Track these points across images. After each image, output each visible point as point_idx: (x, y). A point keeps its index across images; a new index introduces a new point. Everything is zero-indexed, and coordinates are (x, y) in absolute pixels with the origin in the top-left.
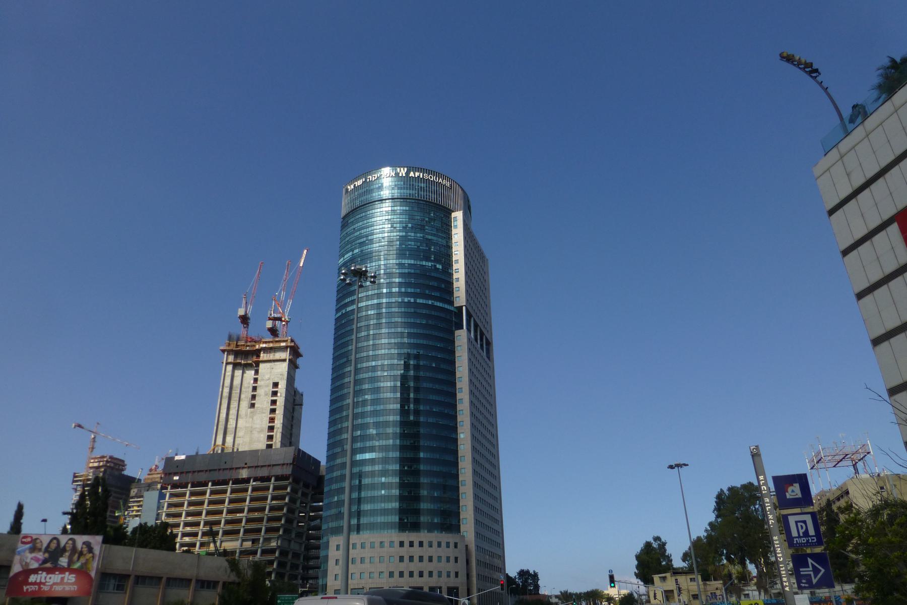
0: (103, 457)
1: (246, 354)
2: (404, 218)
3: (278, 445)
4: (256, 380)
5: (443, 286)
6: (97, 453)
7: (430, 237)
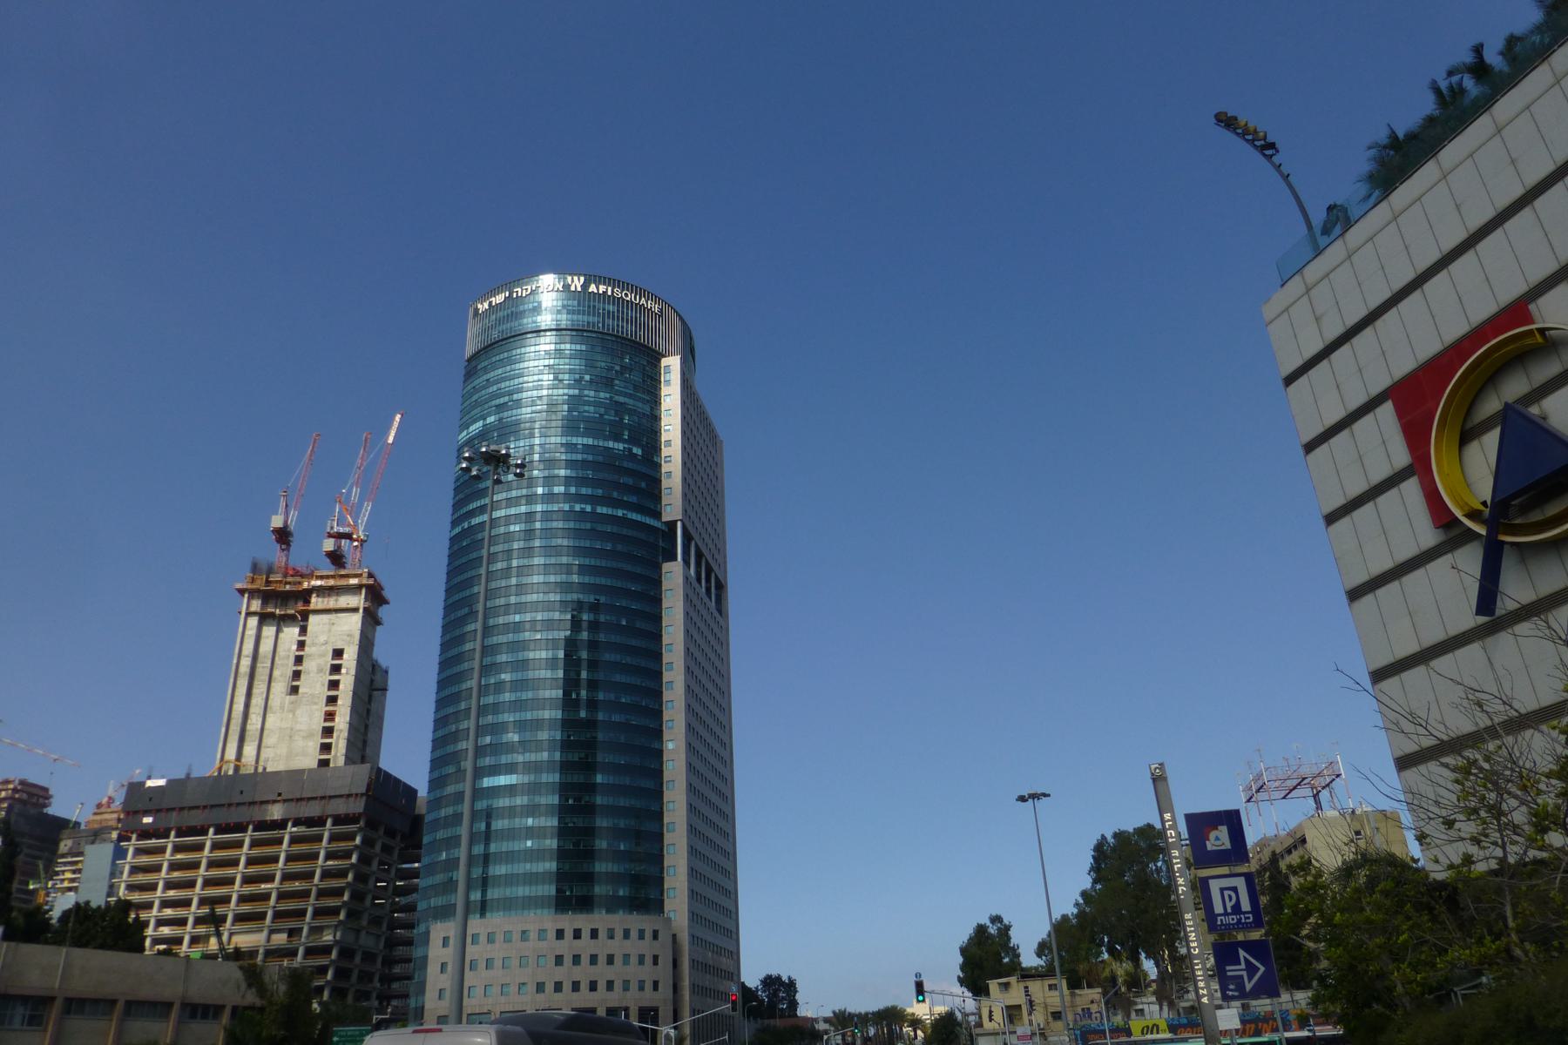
0: (7, 782)
1: (284, 598)
2: (577, 364)
3: (341, 761)
4: (301, 645)
5: (643, 485)
7: (621, 399)
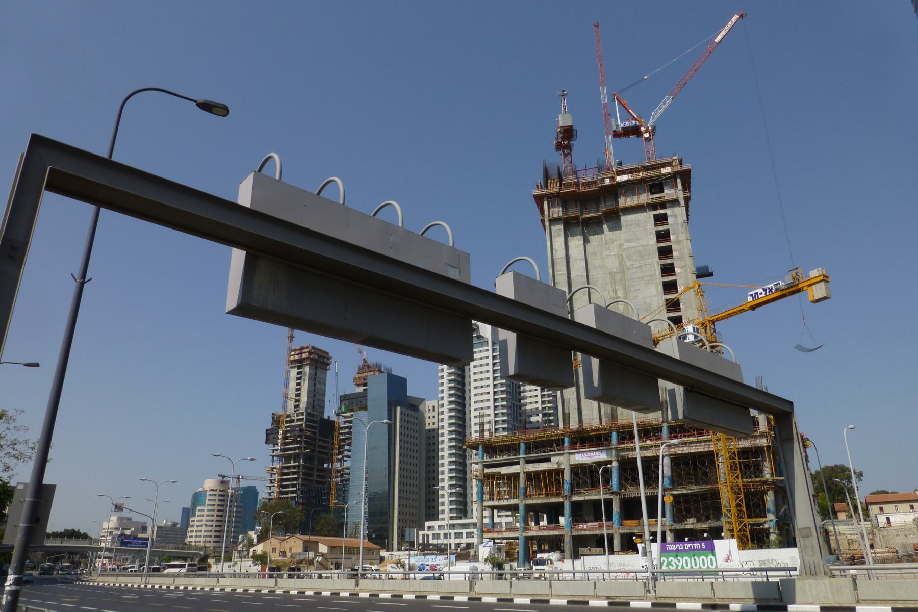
0: (302, 348)
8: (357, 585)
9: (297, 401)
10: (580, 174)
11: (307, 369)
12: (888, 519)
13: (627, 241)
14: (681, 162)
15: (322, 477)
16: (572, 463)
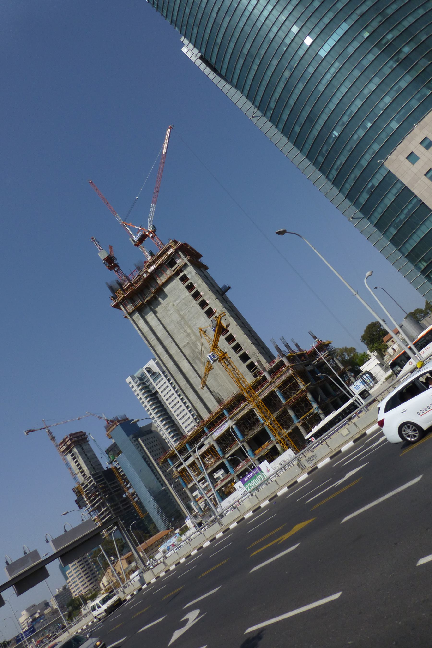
0: (64, 440)
6: (59, 440)
8: (69, 633)
9: (82, 472)
10: (131, 278)
11: (75, 450)
12: (393, 349)
13: (175, 301)
14: (175, 242)
15: (126, 504)
16: (215, 439)
